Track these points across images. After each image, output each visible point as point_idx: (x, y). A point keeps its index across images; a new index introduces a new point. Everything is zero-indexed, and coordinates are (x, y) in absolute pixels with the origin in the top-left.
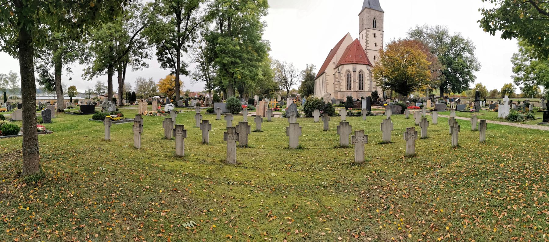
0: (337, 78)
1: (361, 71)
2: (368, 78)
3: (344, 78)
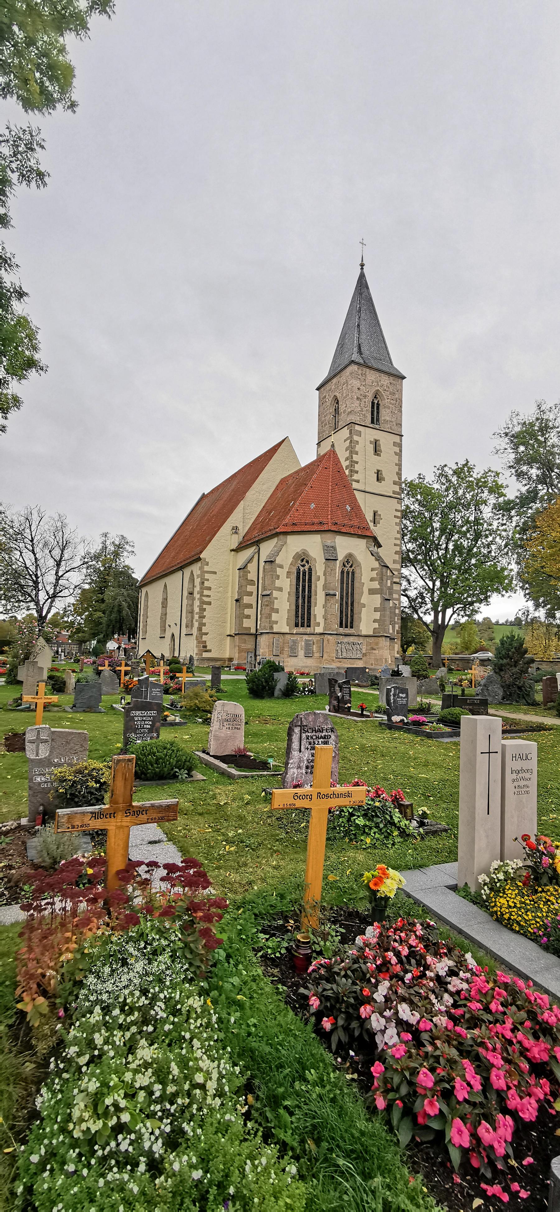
0: (251, 582)
1: (349, 560)
2: (376, 585)
3: (285, 584)
